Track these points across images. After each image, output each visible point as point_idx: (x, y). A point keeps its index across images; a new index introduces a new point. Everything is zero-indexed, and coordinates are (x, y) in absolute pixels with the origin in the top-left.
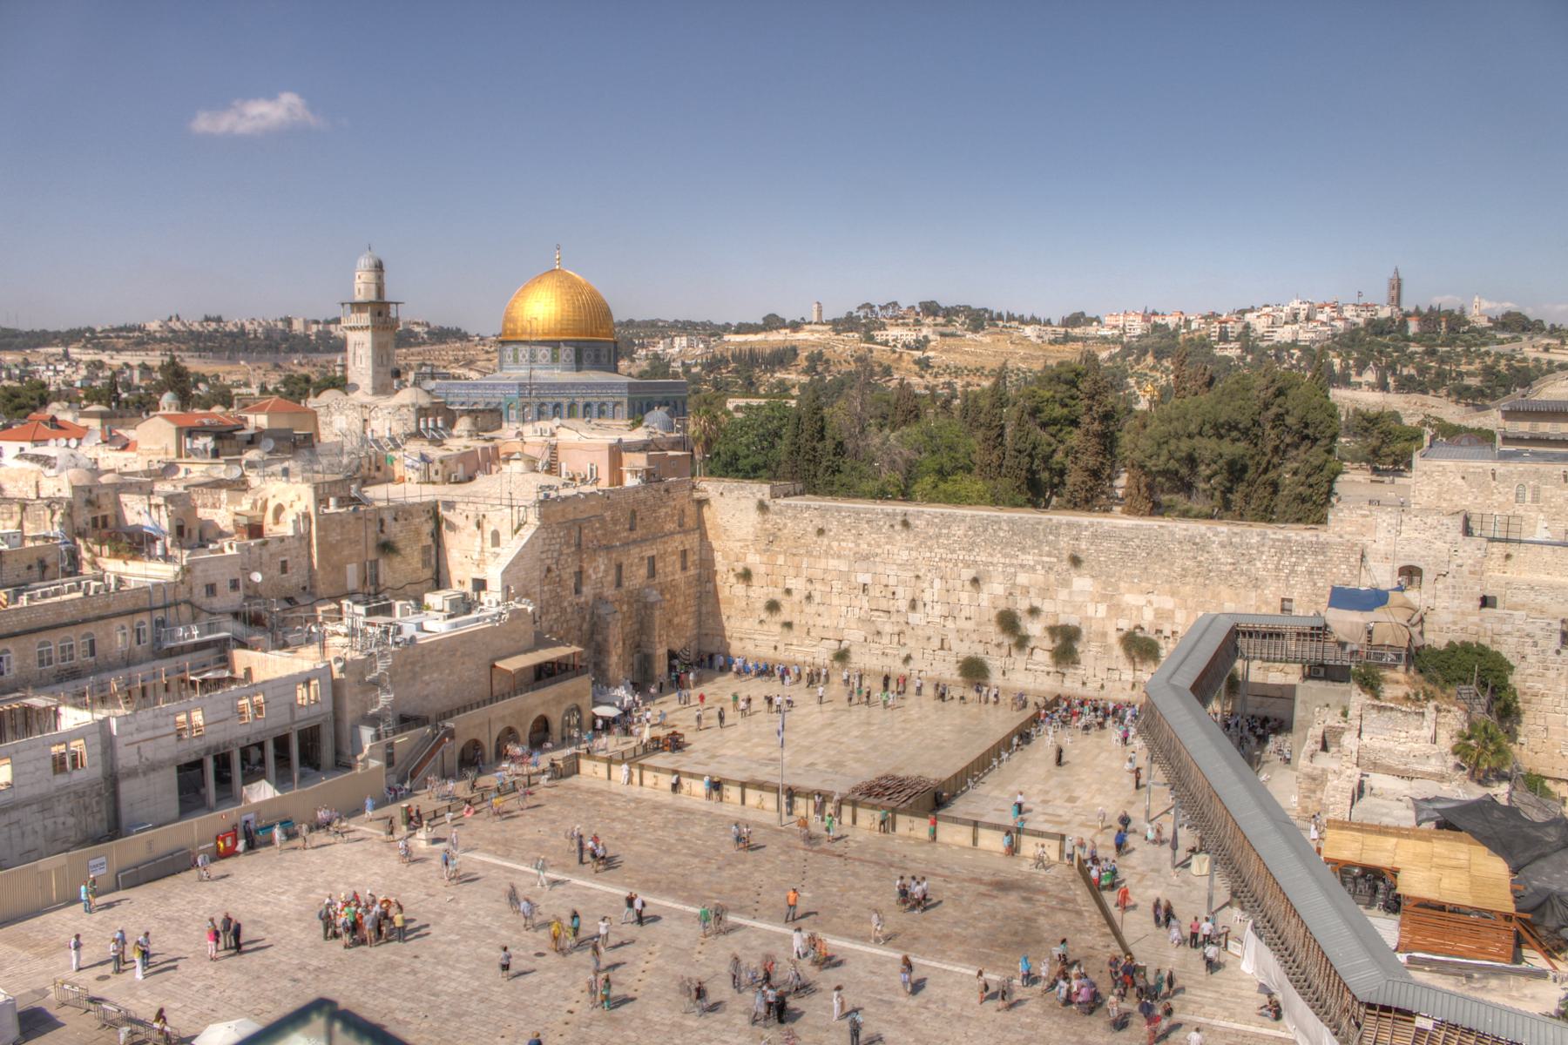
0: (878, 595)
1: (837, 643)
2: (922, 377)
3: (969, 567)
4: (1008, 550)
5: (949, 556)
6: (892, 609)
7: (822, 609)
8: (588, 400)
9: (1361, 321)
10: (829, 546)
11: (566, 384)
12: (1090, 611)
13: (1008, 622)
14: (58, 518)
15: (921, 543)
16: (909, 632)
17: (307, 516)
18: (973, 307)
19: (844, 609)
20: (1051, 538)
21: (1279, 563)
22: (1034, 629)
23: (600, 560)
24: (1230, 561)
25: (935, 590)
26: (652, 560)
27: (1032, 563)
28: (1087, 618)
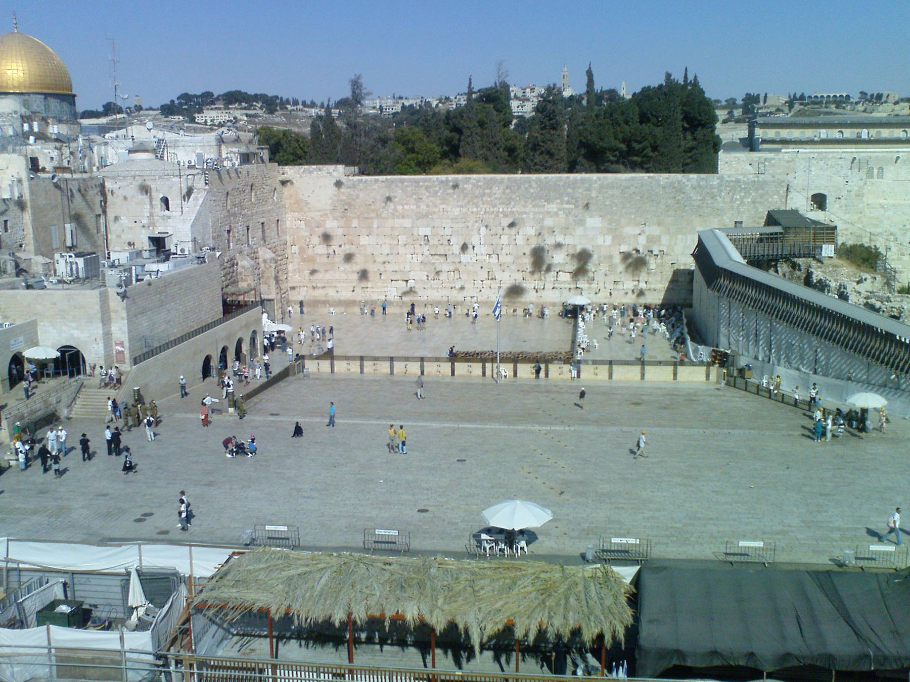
0: (436, 242)
1: (405, 283)
3: (506, 216)
4: (537, 202)
5: (492, 209)
7: (391, 258)
10: (395, 210)
12: (600, 241)
15: (469, 202)
17: (20, 181)
20: (570, 190)
22: (558, 258)
24: (699, 198)
26: (263, 224)
27: (555, 210)
28: (598, 246)
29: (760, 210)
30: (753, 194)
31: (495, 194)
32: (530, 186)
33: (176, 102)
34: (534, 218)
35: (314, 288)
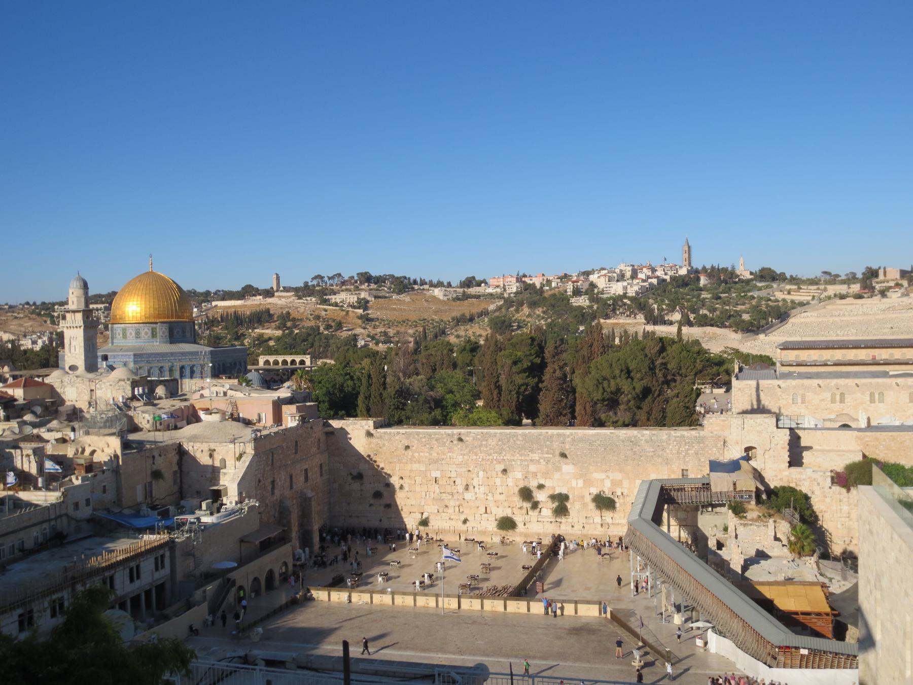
0: (445, 483)
2: (364, 328)
5: (488, 457)
6: (455, 491)
7: (410, 494)
8: (182, 364)
9: (668, 278)
11: (167, 354)
12: (574, 484)
13: (526, 494)
15: (470, 451)
16: (465, 504)
18: (396, 275)
19: (424, 494)
20: (548, 443)
21: (679, 448)
25: (480, 479)
26: (306, 470)
27: (537, 458)
29: (702, 460)
30: (696, 447)
31: (490, 445)
32: (518, 440)
33: (310, 284)
34: (521, 465)
35: (350, 516)
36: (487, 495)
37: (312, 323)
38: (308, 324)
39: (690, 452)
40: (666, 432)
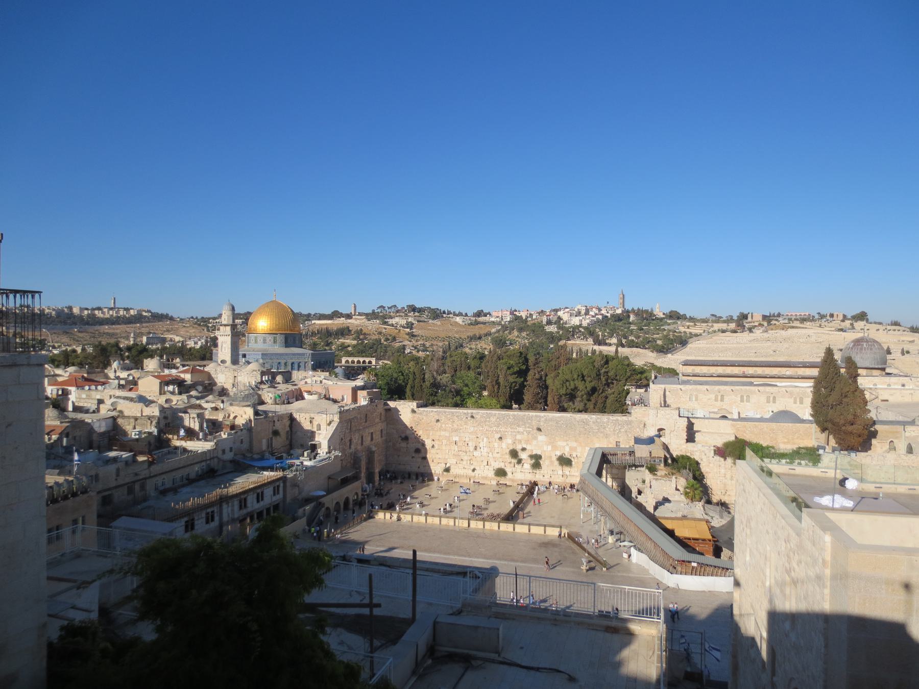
2: (410, 341)
4: (513, 426)
7: (438, 451)
8: (293, 361)
9: (609, 315)
10: (441, 426)
12: (545, 448)
13: (514, 454)
14: (154, 423)
18: (432, 308)
19: (447, 451)
20: (529, 421)
22: (523, 456)
23: (356, 434)
26: (372, 433)
28: (545, 451)
33: (376, 311)
35: (400, 464)
36: (488, 454)
37: (377, 337)
38: (374, 337)
39: (622, 430)
40: (607, 417)
